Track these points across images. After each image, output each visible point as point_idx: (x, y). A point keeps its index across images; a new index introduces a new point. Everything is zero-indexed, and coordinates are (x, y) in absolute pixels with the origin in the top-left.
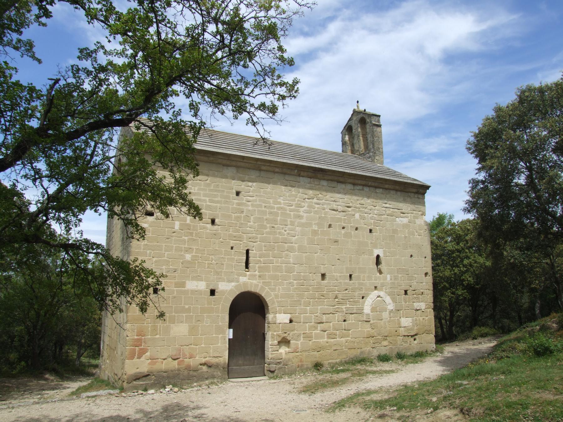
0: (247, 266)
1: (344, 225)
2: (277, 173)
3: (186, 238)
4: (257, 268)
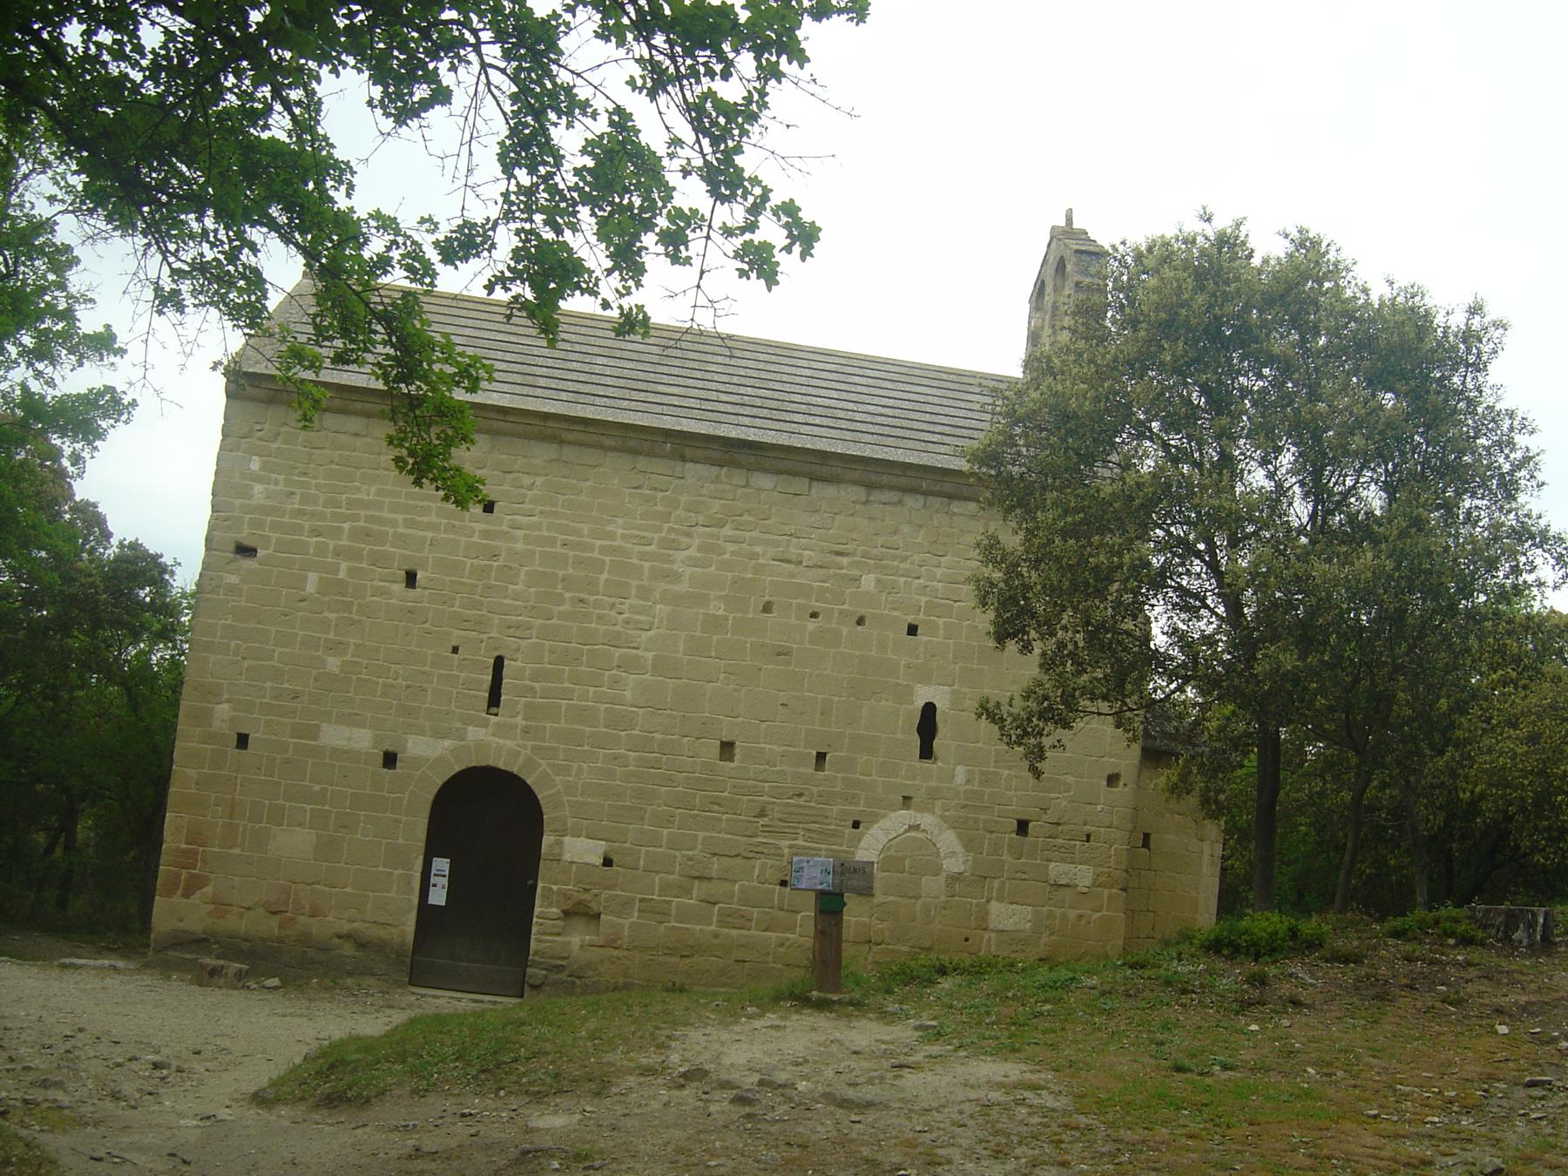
0: (494, 700)
1: (819, 606)
2: (612, 449)
3: (332, 616)
4: (520, 707)
